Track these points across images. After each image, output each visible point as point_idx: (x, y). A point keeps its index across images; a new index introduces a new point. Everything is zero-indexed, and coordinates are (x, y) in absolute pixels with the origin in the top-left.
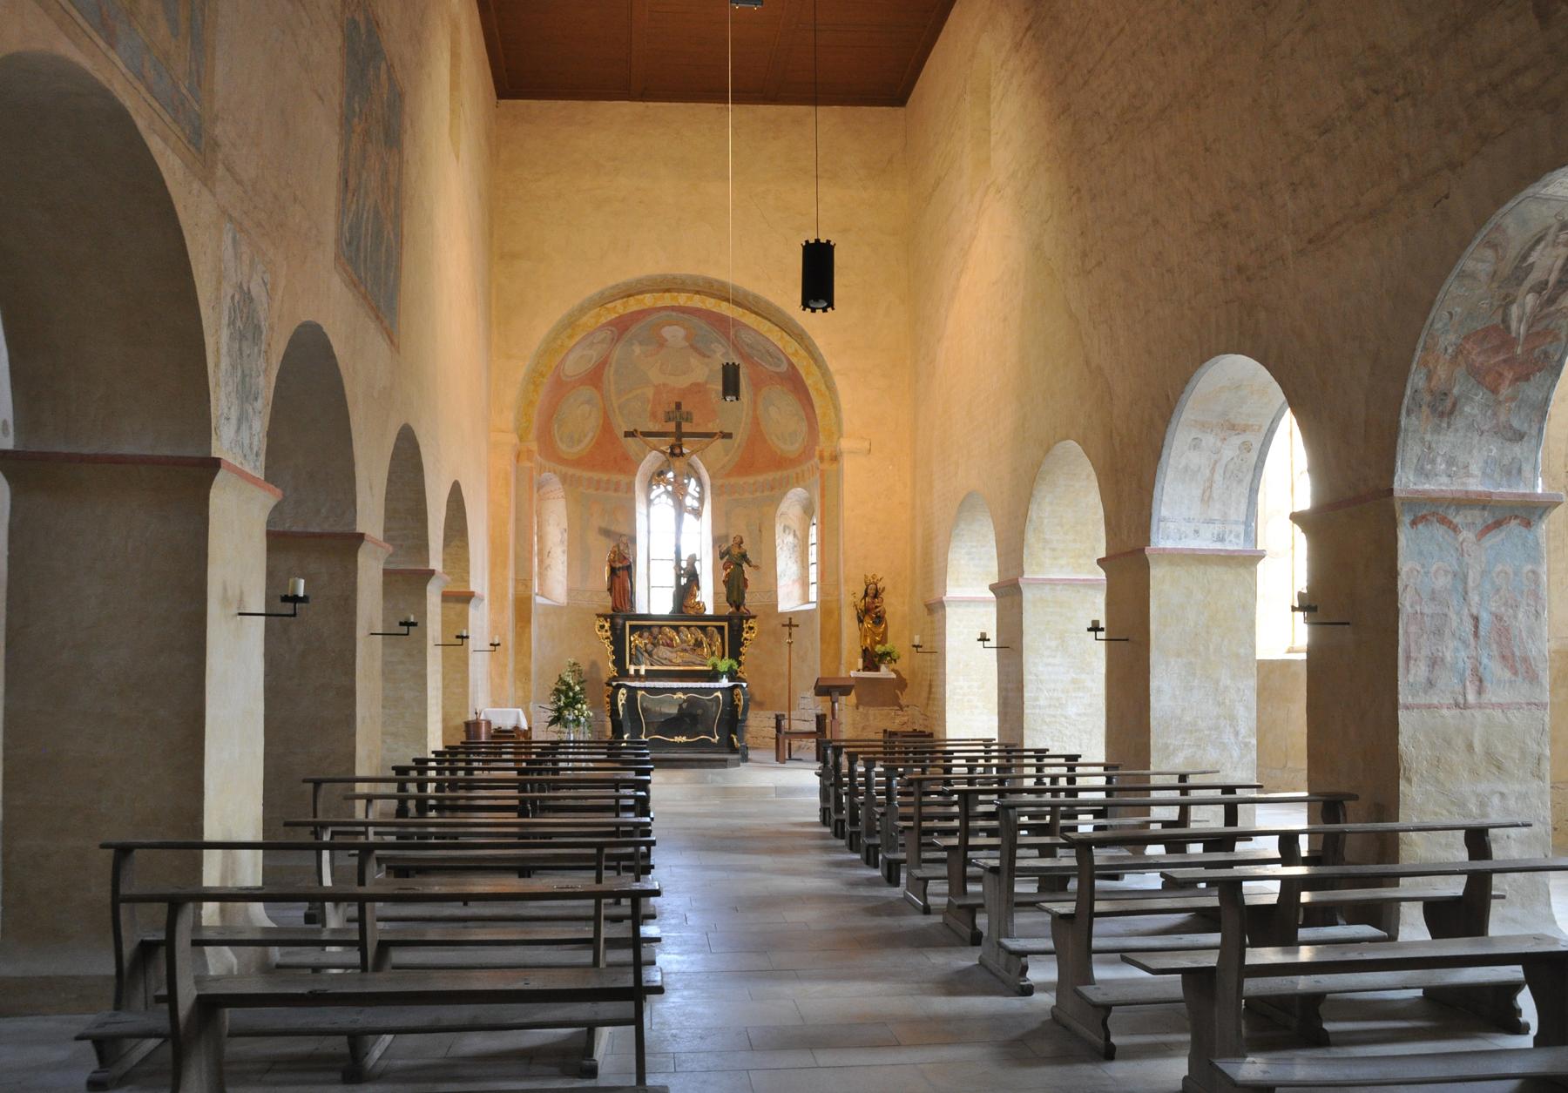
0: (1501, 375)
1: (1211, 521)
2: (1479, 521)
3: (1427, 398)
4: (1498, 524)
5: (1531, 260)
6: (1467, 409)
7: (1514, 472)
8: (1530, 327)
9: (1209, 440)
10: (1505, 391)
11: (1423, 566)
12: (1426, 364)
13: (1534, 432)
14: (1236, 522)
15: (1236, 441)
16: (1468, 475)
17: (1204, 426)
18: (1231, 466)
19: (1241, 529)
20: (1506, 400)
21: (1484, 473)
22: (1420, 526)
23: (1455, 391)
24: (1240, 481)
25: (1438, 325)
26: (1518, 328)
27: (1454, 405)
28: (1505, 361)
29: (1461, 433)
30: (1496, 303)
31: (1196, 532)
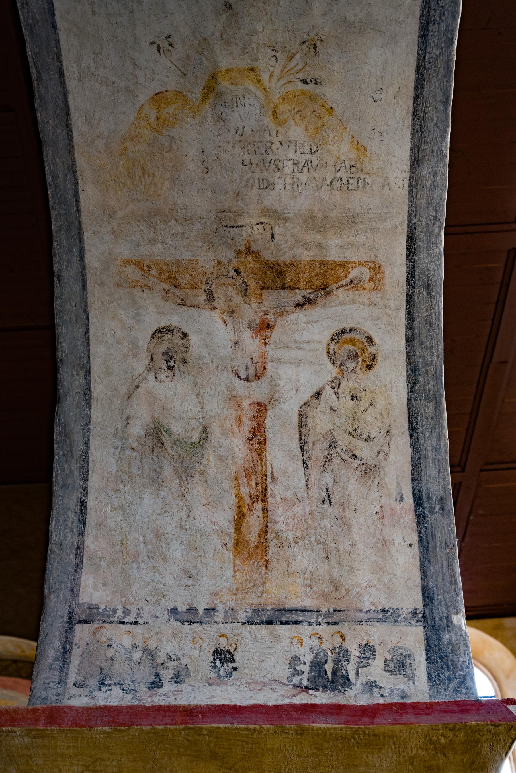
1: (281, 616)
9: (212, 332)
14: (387, 615)
15: (310, 329)
17: (175, 282)
18: (321, 422)
19: (412, 639)
24: (369, 471)
31: (223, 656)
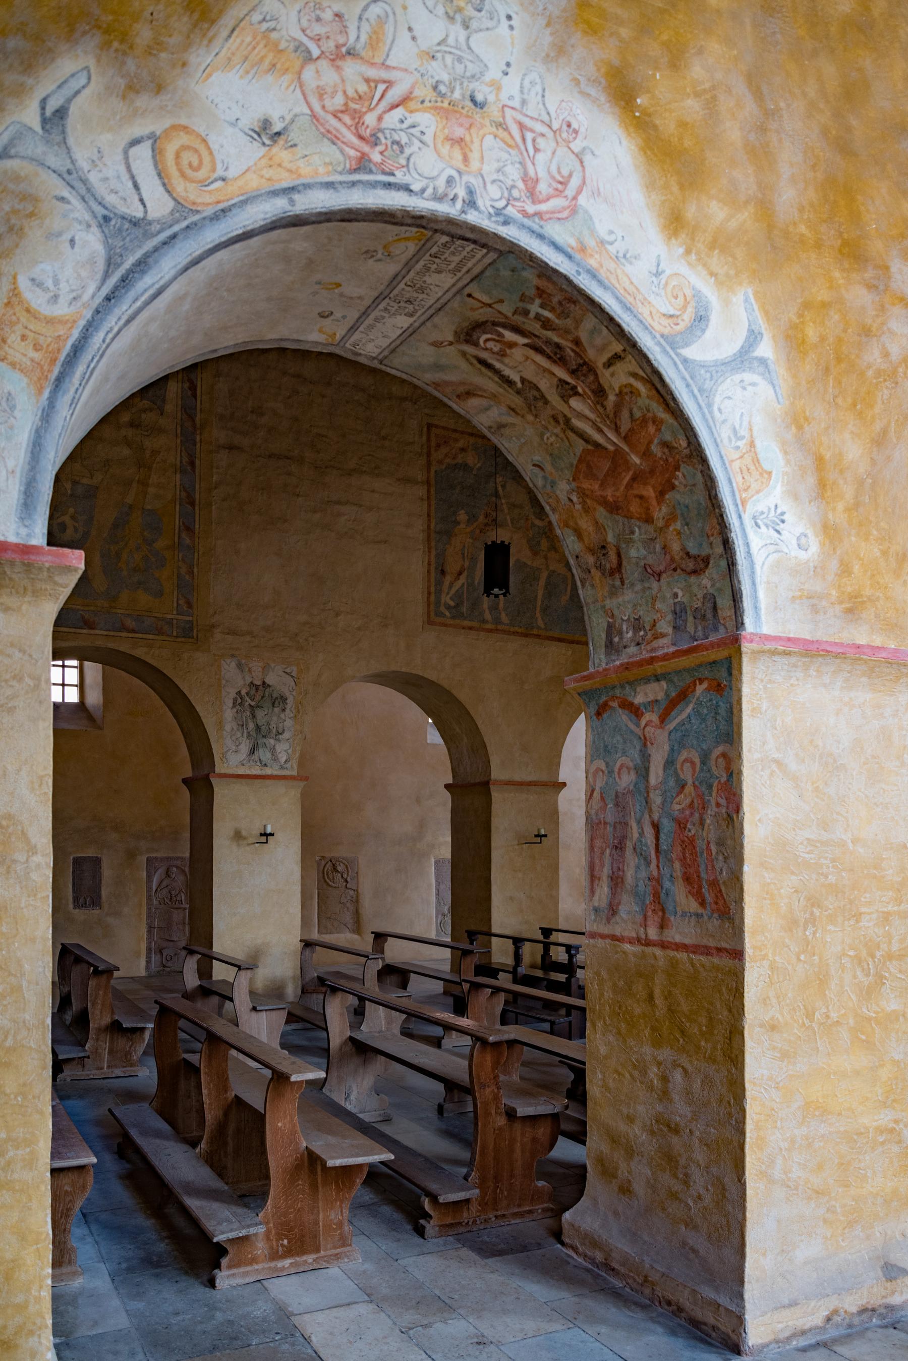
0: (641, 497)
2: (660, 696)
3: (591, 560)
4: (683, 696)
5: (516, 378)
6: (633, 553)
7: (709, 615)
8: (617, 429)
10: (660, 513)
11: (607, 764)
12: (567, 525)
13: (719, 550)
16: (656, 637)
20: (668, 523)
21: (674, 627)
22: (605, 716)
23: (610, 538)
25: (540, 483)
26: (610, 439)
27: (619, 555)
28: (634, 479)
29: (638, 587)
30: (558, 430)
